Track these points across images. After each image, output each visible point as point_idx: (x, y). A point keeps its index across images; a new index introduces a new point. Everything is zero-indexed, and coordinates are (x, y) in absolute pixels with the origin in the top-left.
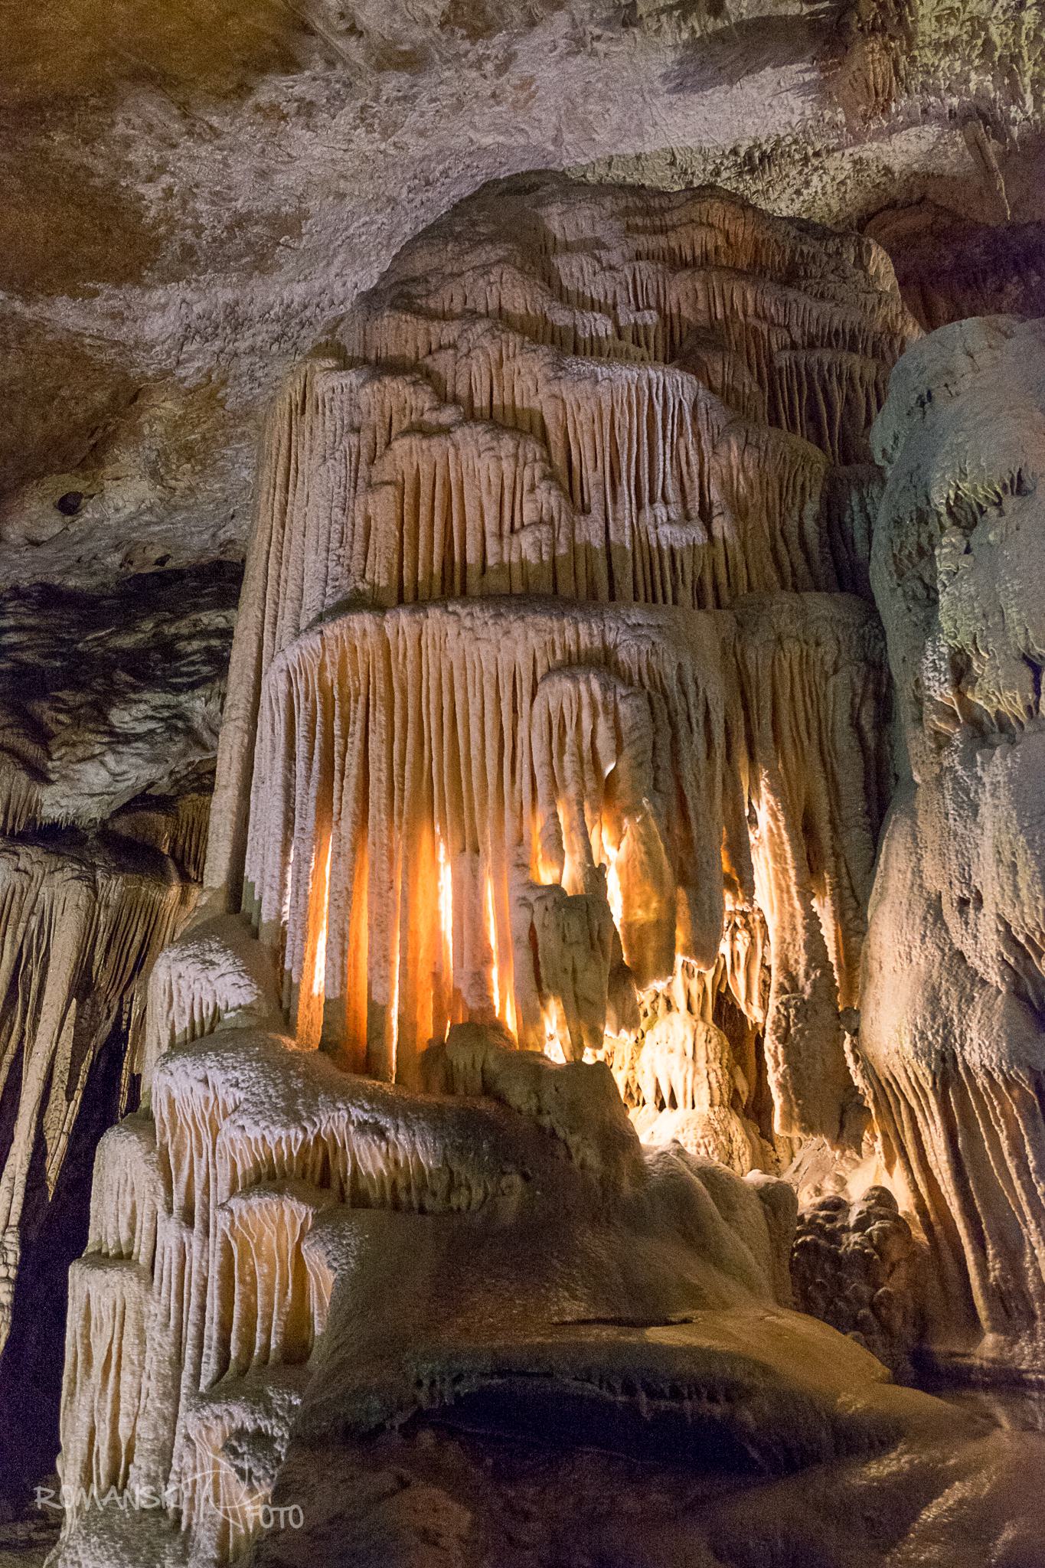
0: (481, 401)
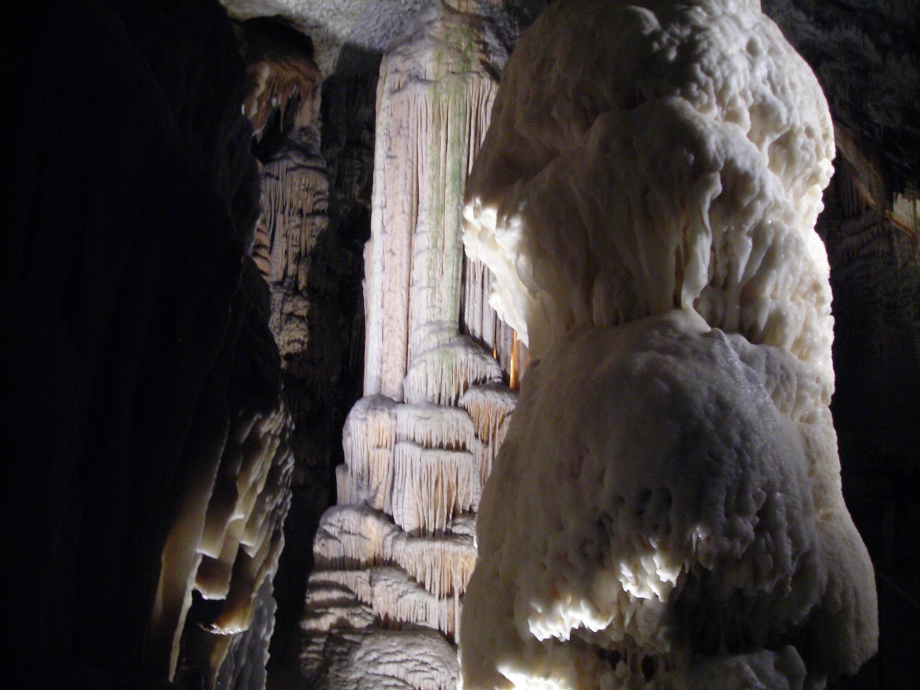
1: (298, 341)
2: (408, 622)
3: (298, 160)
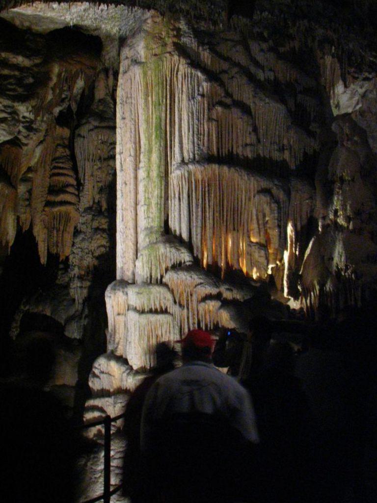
0: (235, 97)
1: (103, 246)
3: (96, 124)
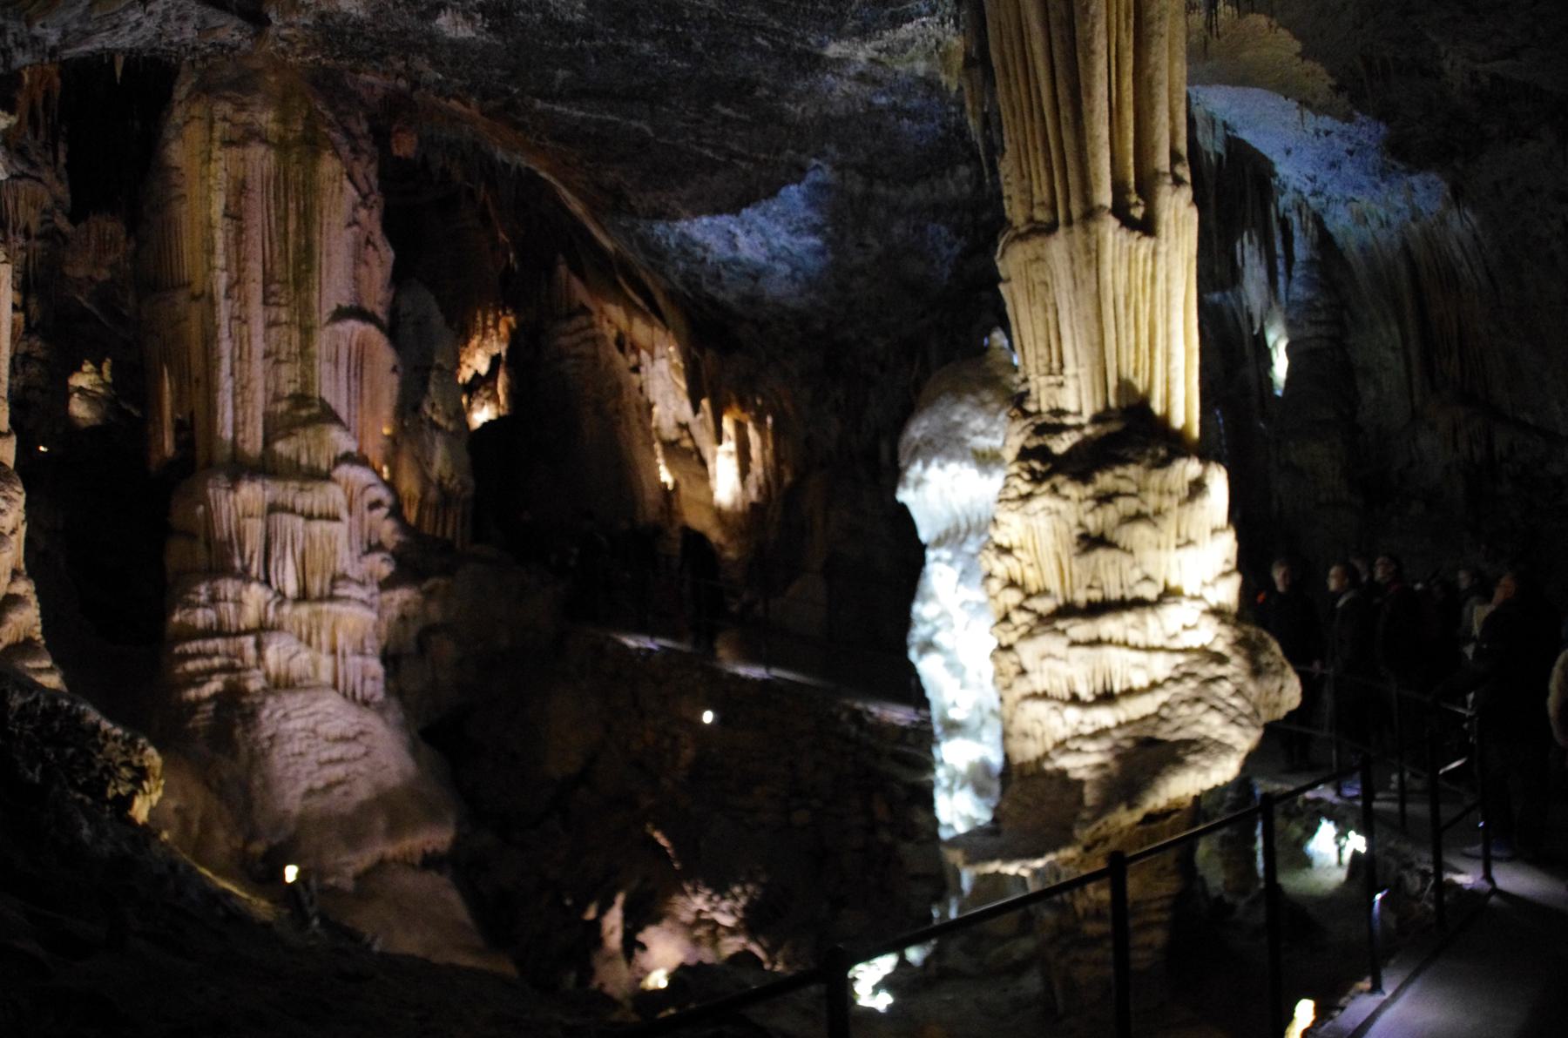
2: (301, 680)
